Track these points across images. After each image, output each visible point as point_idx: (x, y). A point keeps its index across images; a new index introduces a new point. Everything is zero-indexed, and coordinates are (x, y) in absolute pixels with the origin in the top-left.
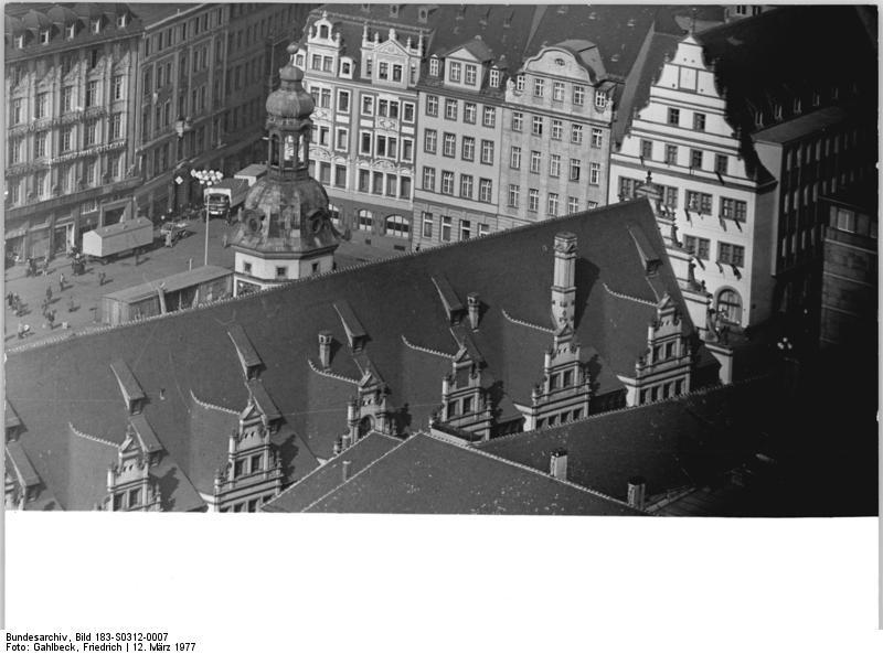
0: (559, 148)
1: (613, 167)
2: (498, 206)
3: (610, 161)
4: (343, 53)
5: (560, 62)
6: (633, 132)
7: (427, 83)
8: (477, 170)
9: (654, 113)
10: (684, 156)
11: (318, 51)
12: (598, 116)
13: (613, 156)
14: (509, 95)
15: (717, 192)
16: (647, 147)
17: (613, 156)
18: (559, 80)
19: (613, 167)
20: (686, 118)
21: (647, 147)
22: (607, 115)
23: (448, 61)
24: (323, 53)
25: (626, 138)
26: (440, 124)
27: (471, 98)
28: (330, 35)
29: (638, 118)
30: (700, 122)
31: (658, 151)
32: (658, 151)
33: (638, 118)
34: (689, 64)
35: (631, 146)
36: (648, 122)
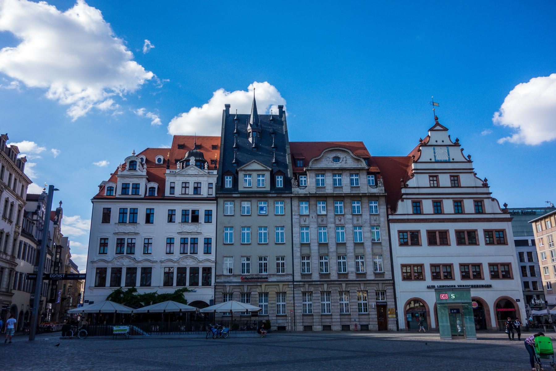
0: (342, 221)
1: (391, 225)
3: (389, 221)
4: (149, 180)
5: (336, 159)
6: (404, 197)
7: (222, 193)
9: (418, 182)
10: (448, 206)
11: (127, 181)
12: (375, 191)
13: (391, 217)
14: (296, 190)
15: (480, 228)
16: (417, 206)
17: (391, 217)
19: (391, 225)
20: (445, 180)
22: (379, 190)
23: (241, 175)
24: (131, 181)
25: (400, 202)
28: (138, 167)
29: (406, 187)
30: (455, 181)
31: (428, 206)
32: (428, 206)
33: (406, 187)
34: (440, 143)
35: (404, 207)
36: (419, 188)
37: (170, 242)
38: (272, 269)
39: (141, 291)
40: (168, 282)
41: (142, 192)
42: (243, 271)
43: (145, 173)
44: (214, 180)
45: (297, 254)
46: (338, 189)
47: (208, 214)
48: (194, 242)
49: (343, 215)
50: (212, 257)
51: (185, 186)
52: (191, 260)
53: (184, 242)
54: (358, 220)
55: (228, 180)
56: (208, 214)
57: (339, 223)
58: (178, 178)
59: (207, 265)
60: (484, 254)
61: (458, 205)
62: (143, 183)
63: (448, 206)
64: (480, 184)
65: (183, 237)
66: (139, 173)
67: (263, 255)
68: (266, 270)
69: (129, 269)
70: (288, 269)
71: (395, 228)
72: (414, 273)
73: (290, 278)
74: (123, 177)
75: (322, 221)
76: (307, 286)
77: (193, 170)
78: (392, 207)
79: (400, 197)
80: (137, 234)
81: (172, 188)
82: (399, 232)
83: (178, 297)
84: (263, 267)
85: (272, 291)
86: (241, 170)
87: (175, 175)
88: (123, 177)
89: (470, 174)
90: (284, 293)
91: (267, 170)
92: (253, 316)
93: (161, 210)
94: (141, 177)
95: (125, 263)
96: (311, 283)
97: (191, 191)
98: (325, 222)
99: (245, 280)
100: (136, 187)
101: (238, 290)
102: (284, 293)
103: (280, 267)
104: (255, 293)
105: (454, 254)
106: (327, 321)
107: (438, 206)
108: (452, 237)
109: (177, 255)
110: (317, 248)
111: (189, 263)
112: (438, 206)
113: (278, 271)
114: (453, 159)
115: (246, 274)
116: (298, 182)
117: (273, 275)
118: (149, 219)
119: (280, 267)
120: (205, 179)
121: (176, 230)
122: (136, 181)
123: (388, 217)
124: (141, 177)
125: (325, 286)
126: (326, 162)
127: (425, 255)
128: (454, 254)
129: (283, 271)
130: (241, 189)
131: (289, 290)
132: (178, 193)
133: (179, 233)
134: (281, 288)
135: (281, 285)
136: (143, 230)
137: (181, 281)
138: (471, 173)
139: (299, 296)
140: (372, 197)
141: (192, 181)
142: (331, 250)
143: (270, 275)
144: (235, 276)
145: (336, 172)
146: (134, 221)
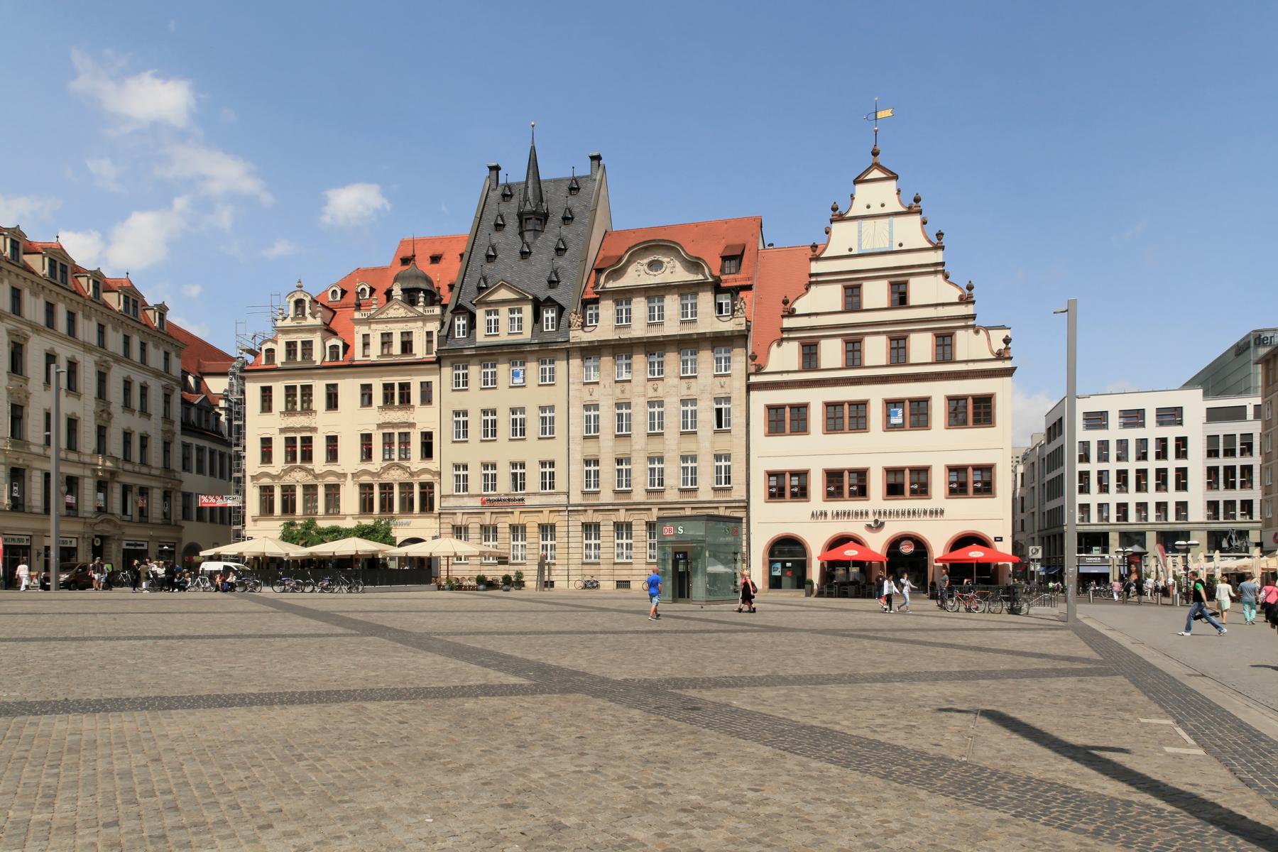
0: (660, 392)
2: (568, 494)
3: (750, 387)
5: (655, 265)
8: (532, 451)
10: (876, 350)
11: (291, 338)
16: (810, 353)
17: (753, 379)
18: (655, 293)
20: (876, 294)
21: (810, 353)
23: (480, 314)
24: (299, 338)
26: (475, 400)
27: (515, 353)
28: (308, 311)
29: (791, 314)
31: (831, 353)
32: (831, 353)
37: (367, 439)
38: (533, 482)
39: (323, 524)
40: (366, 506)
41: (317, 356)
42: (486, 488)
43: (318, 321)
44: (434, 327)
45: (577, 457)
46: (654, 328)
47: (426, 388)
48: (405, 439)
49: (662, 379)
50: (433, 465)
51: (386, 339)
52: (399, 472)
53: (388, 439)
54: (689, 388)
55: (461, 322)
56: (426, 388)
57: (655, 394)
58: (373, 326)
59: (426, 478)
60: (941, 446)
61: (898, 345)
62: (317, 339)
63: (876, 350)
64: (953, 294)
65: (386, 431)
66: (310, 321)
67: (517, 459)
68: (523, 487)
69: (306, 487)
70: (560, 484)
71: (761, 399)
72: (789, 486)
73: (562, 499)
74: (285, 331)
75: (623, 392)
76: (590, 512)
77: (397, 311)
80: (314, 430)
81: (366, 345)
82: (770, 408)
83: (379, 533)
84: (518, 481)
85: (532, 522)
86: (481, 303)
87: (368, 321)
88: (285, 331)
89: (931, 278)
90: (553, 527)
91: (523, 300)
92: (500, 563)
93: (349, 388)
94: (312, 329)
95: (298, 478)
96: (598, 509)
97: (396, 348)
98: (627, 395)
99: (488, 502)
100: (307, 345)
101: (477, 520)
102: (553, 527)
103: (548, 482)
104: (503, 524)
106: (623, 574)
107: (853, 348)
108: (876, 414)
109: (377, 462)
110: (611, 443)
111: (395, 476)
112: (853, 348)
113: (544, 486)
114: (901, 245)
115: (490, 492)
116: (584, 317)
117: (534, 494)
118: (332, 401)
119: (548, 482)
120: (420, 324)
121: (371, 419)
122: (306, 337)
123: (748, 378)
124: (312, 329)
125: (622, 512)
126: (636, 275)
128: (876, 450)
129: (552, 486)
130: (481, 336)
131: (559, 520)
132: (375, 353)
133: (380, 426)
134: (545, 518)
135: (546, 511)
136: (323, 422)
137: (387, 505)
138: (936, 272)
139: (577, 530)
140: (719, 341)
141: (397, 330)
142: (636, 447)
143: (528, 494)
144: (473, 496)
145: (652, 293)
146: (308, 410)
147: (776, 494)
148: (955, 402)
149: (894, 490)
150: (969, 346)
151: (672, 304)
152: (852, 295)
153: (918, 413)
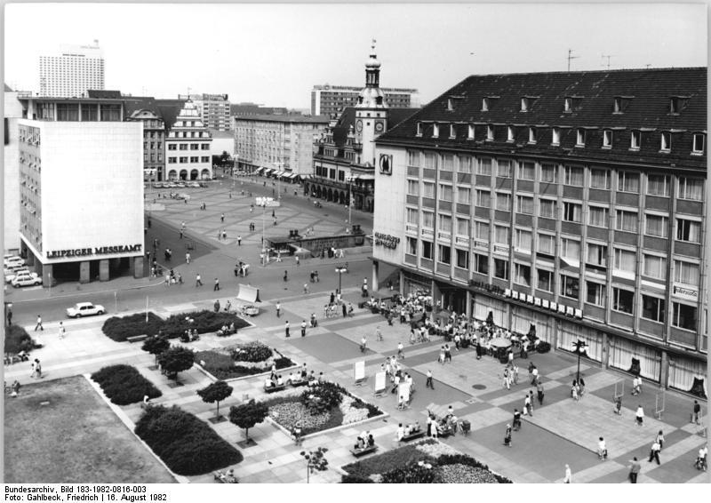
9: (179, 124)
10: (189, 135)
15: (200, 143)
18: (146, 120)
20: (189, 124)
21: (177, 133)
22: (163, 127)
32: (181, 135)
35: (172, 135)
63: (189, 135)
71: (167, 143)
72: (173, 160)
78: (167, 134)
79: (171, 130)
105: (189, 153)
127: (178, 154)
128: (189, 153)
147: (170, 162)
148: (203, 145)
149: (181, 161)
150: (205, 135)
151: (149, 123)
152: (185, 123)
153: (196, 147)
